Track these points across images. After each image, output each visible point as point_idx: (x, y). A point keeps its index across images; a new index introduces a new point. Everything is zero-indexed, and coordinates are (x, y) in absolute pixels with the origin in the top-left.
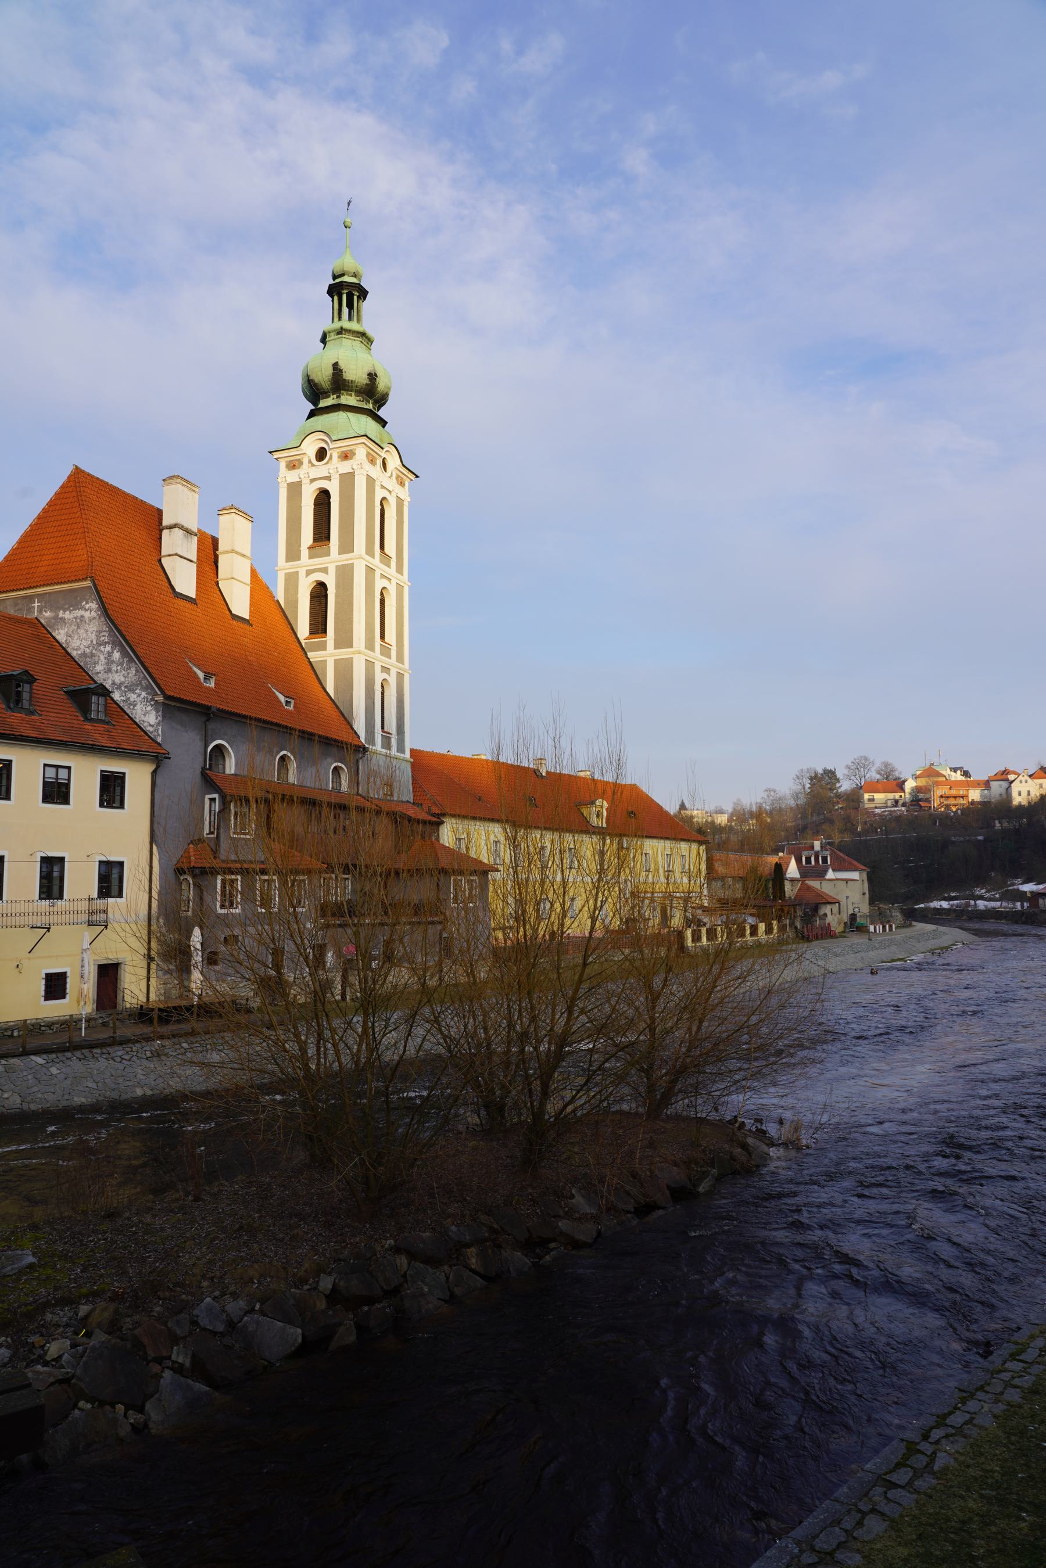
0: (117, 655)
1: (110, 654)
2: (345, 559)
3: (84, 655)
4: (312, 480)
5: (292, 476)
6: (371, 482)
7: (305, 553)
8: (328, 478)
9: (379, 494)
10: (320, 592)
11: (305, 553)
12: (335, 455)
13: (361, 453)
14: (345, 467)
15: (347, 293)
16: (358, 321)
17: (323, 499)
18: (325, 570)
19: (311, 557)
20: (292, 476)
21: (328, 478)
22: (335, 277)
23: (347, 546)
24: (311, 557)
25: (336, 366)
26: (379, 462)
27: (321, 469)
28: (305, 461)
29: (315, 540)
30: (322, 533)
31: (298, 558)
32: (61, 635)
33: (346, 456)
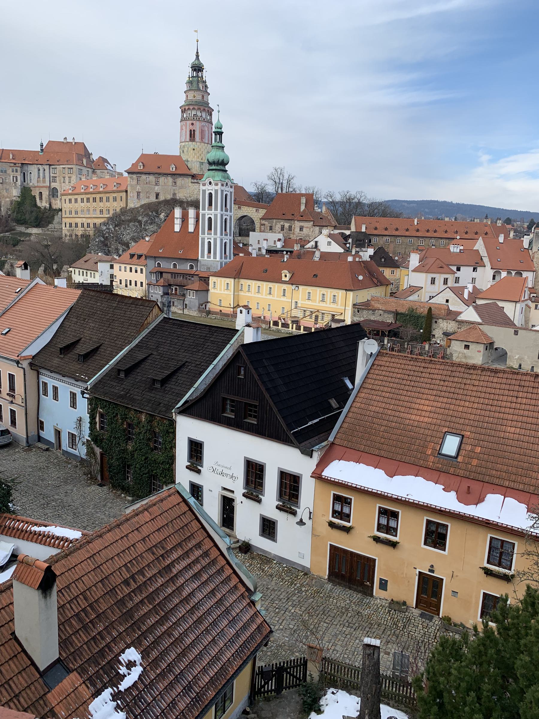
5: (204, 188)
6: (222, 191)
7: (206, 209)
9: (225, 193)
11: (206, 209)
13: (220, 184)
14: (216, 188)
16: (221, 142)
17: (210, 195)
19: (208, 210)
20: (204, 188)
23: (216, 209)
24: (208, 210)
26: (225, 184)
27: (210, 187)
30: (210, 204)
31: (205, 210)
33: (216, 185)
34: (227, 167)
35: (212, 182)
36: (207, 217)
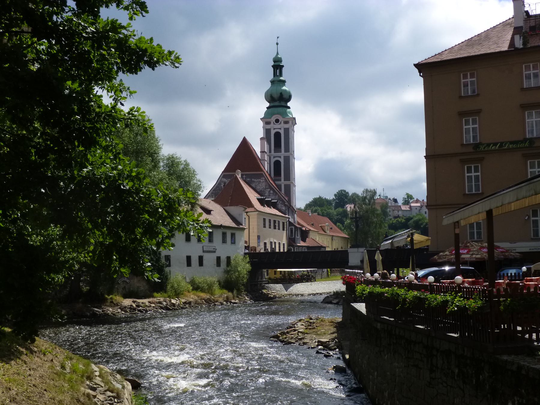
0: (272, 192)
1: (269, 191)
2: (287, 154)
3: (261, 191)
4: (274, 129)
5: (268, 127)
8: (280, 129)
10: (277, 164)
12: (282, 122)
14: (286, 126)
15: (278, 66)
18: (280, 157)
19: (275, 152)
20: (268, 127)
21: (280, 129)
22: (274, 62)
24: (275, 152)
25: (281, 94)
27: (277, 126)
28: (272, 123)
29: (275, 147)
32: (253, 185)
34: (289, 104)
35: (281, 119)
36: (273, 160)
